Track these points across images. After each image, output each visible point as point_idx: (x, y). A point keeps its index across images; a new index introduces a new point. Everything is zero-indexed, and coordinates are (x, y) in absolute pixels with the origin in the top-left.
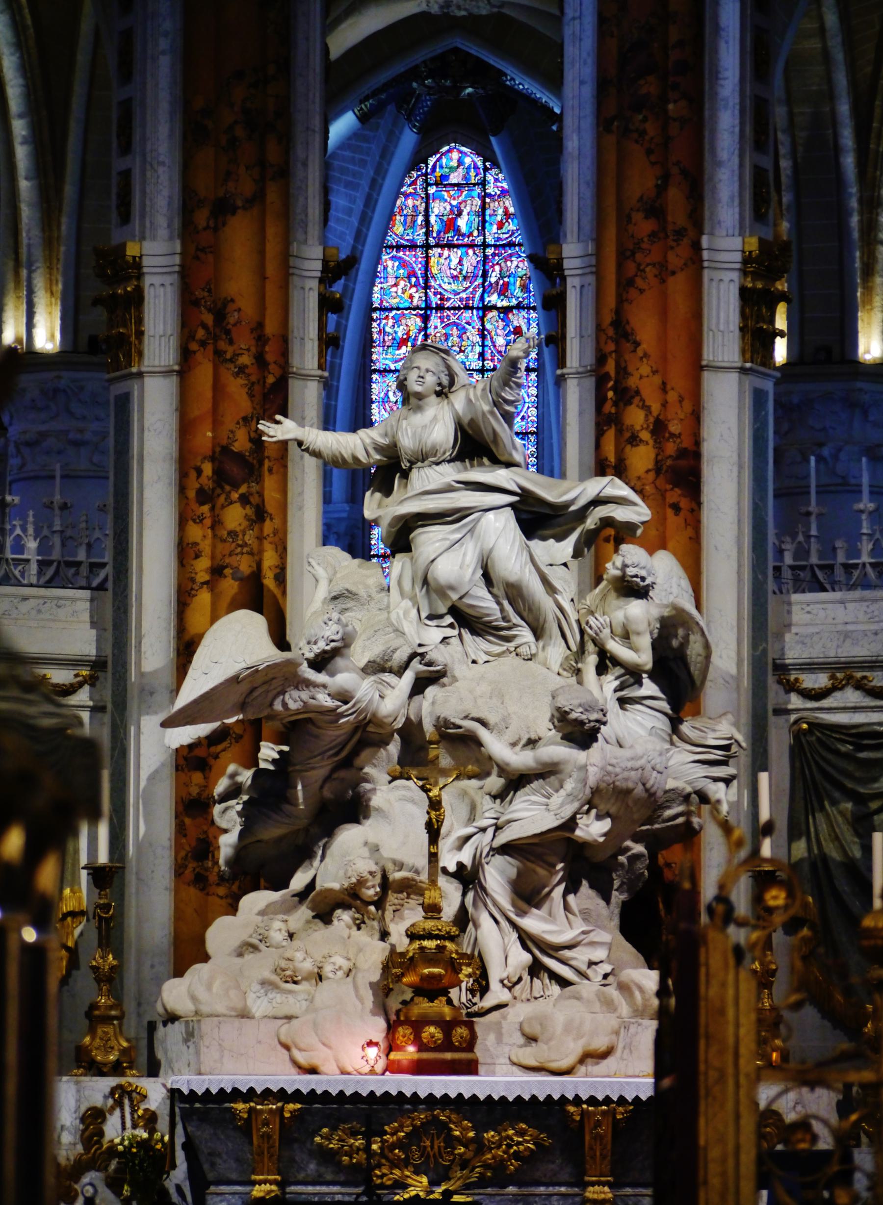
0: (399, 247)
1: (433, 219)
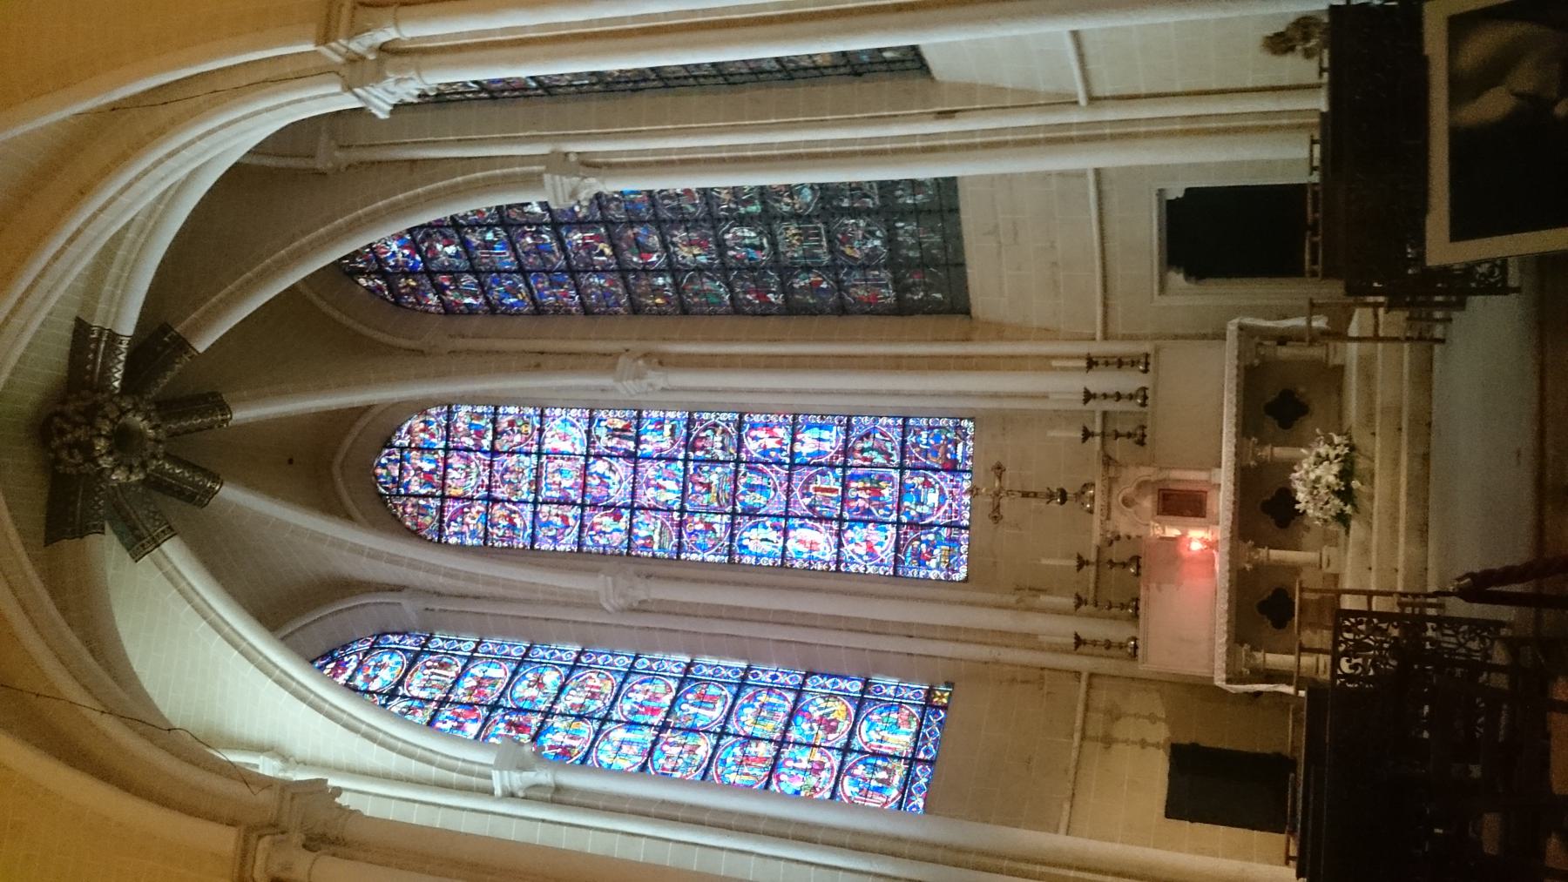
0: (441, 521)
1: (423, 491)
